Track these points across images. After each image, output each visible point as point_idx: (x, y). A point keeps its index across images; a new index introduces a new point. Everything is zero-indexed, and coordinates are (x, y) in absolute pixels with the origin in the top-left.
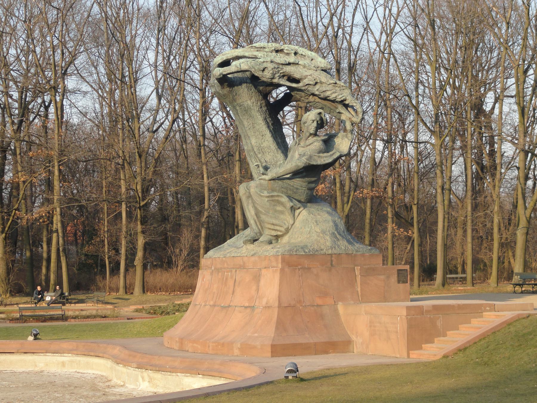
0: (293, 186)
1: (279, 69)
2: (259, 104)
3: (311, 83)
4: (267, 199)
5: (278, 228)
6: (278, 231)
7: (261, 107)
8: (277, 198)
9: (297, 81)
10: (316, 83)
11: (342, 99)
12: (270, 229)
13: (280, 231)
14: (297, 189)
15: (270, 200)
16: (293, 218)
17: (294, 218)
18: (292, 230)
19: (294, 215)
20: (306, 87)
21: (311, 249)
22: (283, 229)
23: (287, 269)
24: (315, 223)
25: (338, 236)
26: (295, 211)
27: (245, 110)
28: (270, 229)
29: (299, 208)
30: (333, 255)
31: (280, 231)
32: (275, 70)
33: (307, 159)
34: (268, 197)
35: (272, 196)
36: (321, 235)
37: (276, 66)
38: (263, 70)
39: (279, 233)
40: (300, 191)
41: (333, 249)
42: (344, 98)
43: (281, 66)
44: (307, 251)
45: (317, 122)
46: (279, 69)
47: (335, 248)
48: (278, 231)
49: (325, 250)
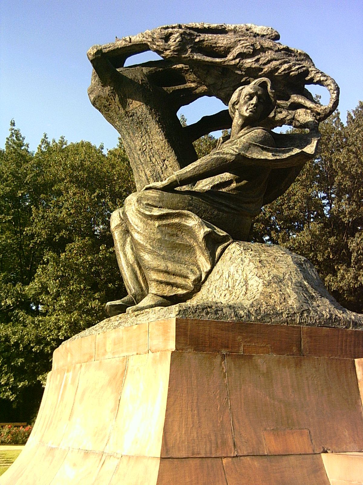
4: (157, 224)
5: (179, 280)
6: (178, 286)
8: (176, 220)
13: (183, 287)
15: (165, 225)
18: (207, 283)
20: (237, 60)
21: (252, 310)
22: (189, 283)
31: (183, 287)
39: (181, 292)
42: (304, 69)
43: (196, 33)
48: (178, 286)
49: (285, 316)
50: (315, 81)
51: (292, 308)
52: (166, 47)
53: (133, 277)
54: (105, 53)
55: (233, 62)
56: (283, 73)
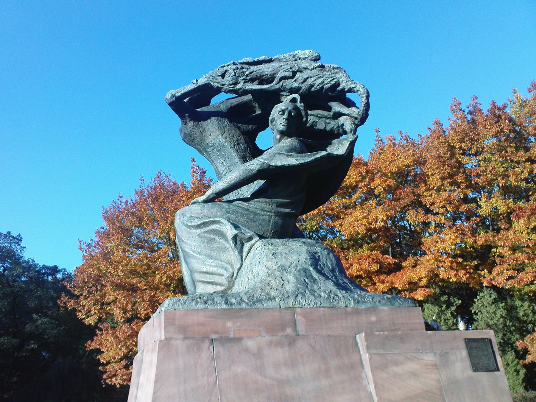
0: (248, 210)
1: (244, 70)
2: (235, 139)
3: (287, 74)
4: (199, 231)
5: (216, 279)
7: (238, 144)
8: (214, 227)
9: (270, 80)
10: (294, 73)
11: (333, 82)
12: (203, 282)
13: (220, 285)
14: (255, 214)
16: (239, 257)
17: (242, 257)
18: (238, 278)
19: (241, 252)
23: (179, 344)
24: (271, 257)
25: (315, 275)
26: (242, 245)
27: (218, 151)
28: (203, 282)
29: (250, 239)
30: (298, 310)
31: (220, 285)
32: (238, 71)
33: (266, 159)
34: (199, 226)
35: (205, 224)
36: (277, 273)
37: (239, 67)
38: (223, 76)
40: (261, 217)
41: (300, 297)
43: (247, 66)
44: (233, 301)
45: (290, 112)
46: (244, 70)
47: (304, 295)
48: (217, 284)
49: (277, 300)
50: (346, 89)
51: (287, 292)
52: (224, 83)
53: (191, 280)
54: (178, 97)
55: (277, 86)
56: (318, 88)
